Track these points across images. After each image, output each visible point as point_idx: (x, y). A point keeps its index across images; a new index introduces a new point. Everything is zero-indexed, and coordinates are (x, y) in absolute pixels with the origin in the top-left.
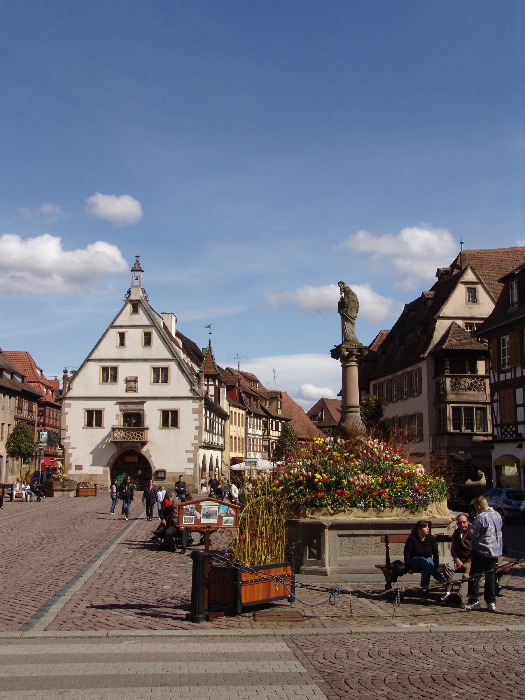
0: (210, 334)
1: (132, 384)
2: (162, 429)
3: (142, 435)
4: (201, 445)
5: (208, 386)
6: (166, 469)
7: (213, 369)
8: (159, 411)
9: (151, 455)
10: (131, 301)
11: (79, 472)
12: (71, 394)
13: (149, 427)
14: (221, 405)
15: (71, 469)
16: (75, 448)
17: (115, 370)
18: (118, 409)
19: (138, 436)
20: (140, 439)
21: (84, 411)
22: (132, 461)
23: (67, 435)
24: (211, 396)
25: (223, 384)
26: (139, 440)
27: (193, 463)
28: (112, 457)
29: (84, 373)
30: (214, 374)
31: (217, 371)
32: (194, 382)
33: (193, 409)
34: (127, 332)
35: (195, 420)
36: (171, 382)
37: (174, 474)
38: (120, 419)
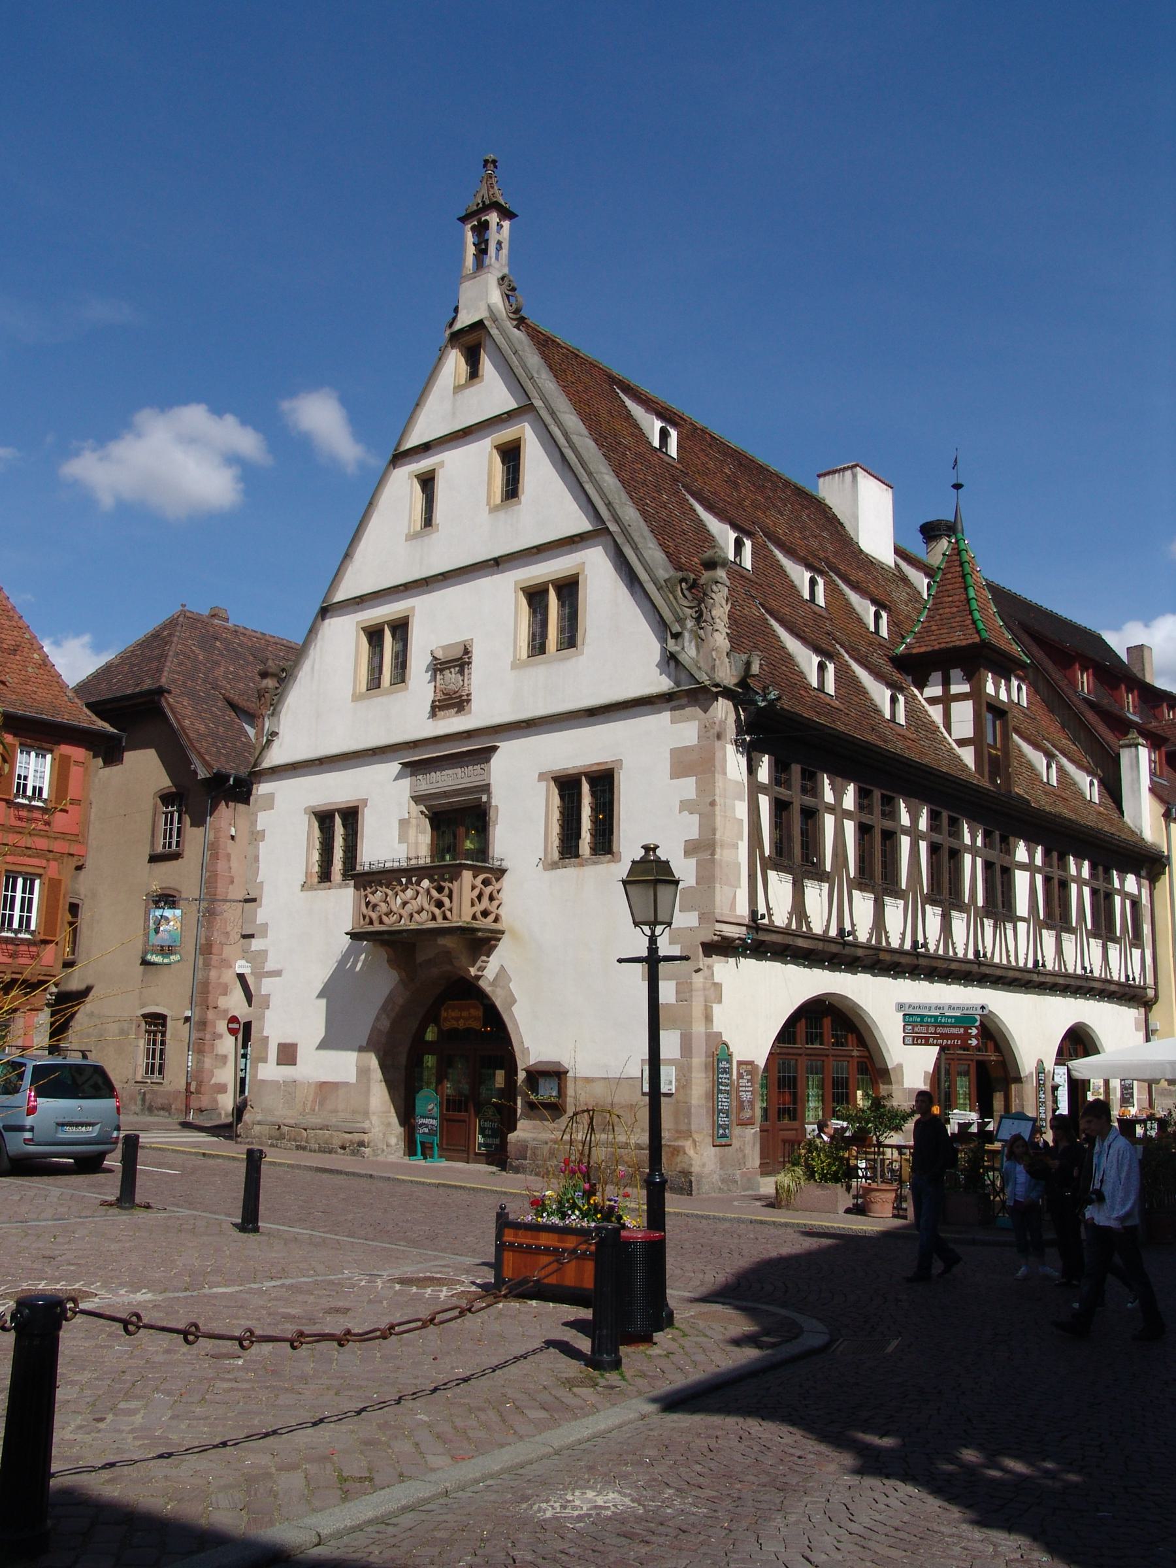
0: (957, 487)
1: (451, 677)
2: (554, 866)
3: (450, 897)
4: (709, 937)
5: (946, 700)
6: (566, 1063)
7: (963, 627)
8: (544, 784)
9: (512, 995)
10: (456, 338)
11: (286, 1072)
12: (276, 756)
13: (505, 865)
14: (1127, 818)
15: (264, 1060)
16: (277, 973)
17: (401, 628)
18: (407, 794)
19: (440, 904)
20: (445, 918)
21: (306, 818)
22: (461, 1025)
23: (258, 923)
24: (962, 743)
25: (1133, 734)
26: (440, 923)
27: (678, 1033)
28: (384, 1008)
29: (313, 668)
30: (964, 643)
31: (978, 632)
32: (681, 621)
33: (674, 752)
34: (442, 464)
35: (685, 806)
36: (588, 641)
37: (599, 1090)
38: (412, 839)
